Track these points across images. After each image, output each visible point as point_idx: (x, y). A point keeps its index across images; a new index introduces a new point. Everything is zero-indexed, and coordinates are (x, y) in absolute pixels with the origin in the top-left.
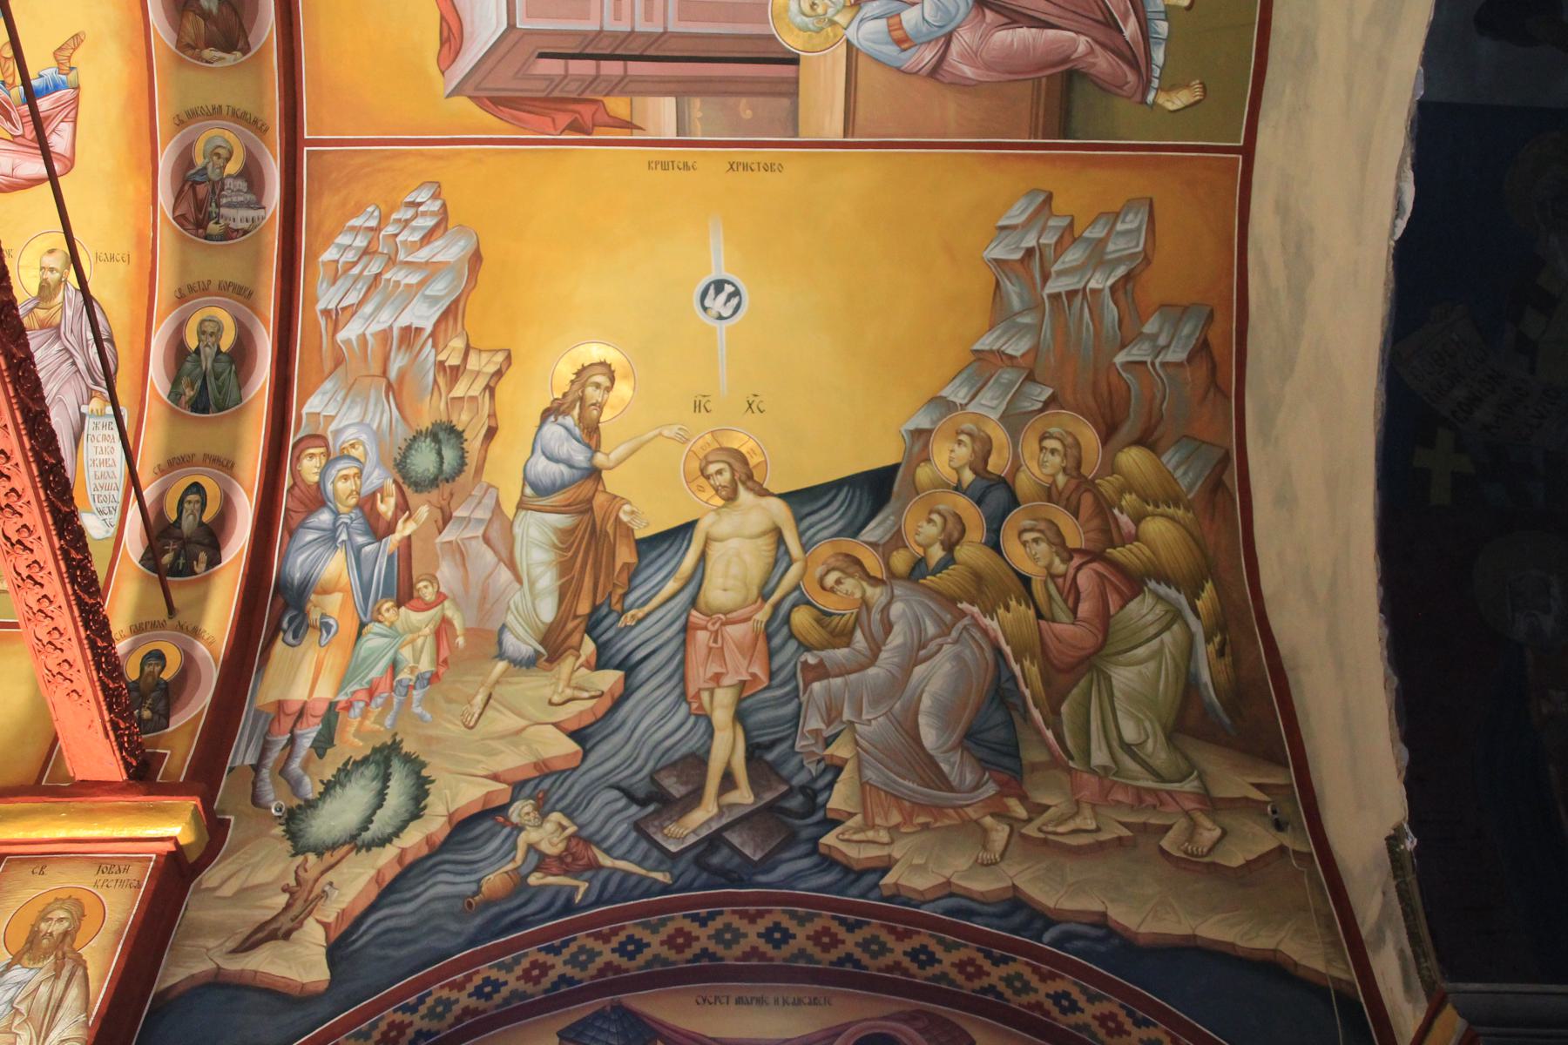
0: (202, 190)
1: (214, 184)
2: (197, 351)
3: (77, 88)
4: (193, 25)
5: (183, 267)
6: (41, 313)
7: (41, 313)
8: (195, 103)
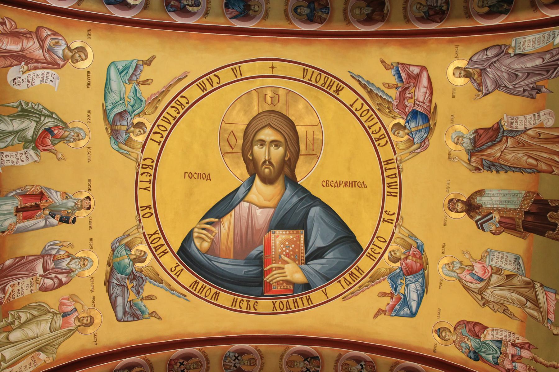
0: (431, 13)
1: (429, 9)
2: (489, 7)
3: (398, 63)
4: (376, 16)
5: (459, 17)
6: (476, 76)
7: (476, 76)
8: (401, 16)
